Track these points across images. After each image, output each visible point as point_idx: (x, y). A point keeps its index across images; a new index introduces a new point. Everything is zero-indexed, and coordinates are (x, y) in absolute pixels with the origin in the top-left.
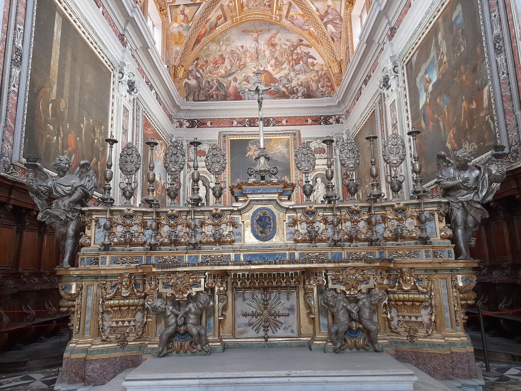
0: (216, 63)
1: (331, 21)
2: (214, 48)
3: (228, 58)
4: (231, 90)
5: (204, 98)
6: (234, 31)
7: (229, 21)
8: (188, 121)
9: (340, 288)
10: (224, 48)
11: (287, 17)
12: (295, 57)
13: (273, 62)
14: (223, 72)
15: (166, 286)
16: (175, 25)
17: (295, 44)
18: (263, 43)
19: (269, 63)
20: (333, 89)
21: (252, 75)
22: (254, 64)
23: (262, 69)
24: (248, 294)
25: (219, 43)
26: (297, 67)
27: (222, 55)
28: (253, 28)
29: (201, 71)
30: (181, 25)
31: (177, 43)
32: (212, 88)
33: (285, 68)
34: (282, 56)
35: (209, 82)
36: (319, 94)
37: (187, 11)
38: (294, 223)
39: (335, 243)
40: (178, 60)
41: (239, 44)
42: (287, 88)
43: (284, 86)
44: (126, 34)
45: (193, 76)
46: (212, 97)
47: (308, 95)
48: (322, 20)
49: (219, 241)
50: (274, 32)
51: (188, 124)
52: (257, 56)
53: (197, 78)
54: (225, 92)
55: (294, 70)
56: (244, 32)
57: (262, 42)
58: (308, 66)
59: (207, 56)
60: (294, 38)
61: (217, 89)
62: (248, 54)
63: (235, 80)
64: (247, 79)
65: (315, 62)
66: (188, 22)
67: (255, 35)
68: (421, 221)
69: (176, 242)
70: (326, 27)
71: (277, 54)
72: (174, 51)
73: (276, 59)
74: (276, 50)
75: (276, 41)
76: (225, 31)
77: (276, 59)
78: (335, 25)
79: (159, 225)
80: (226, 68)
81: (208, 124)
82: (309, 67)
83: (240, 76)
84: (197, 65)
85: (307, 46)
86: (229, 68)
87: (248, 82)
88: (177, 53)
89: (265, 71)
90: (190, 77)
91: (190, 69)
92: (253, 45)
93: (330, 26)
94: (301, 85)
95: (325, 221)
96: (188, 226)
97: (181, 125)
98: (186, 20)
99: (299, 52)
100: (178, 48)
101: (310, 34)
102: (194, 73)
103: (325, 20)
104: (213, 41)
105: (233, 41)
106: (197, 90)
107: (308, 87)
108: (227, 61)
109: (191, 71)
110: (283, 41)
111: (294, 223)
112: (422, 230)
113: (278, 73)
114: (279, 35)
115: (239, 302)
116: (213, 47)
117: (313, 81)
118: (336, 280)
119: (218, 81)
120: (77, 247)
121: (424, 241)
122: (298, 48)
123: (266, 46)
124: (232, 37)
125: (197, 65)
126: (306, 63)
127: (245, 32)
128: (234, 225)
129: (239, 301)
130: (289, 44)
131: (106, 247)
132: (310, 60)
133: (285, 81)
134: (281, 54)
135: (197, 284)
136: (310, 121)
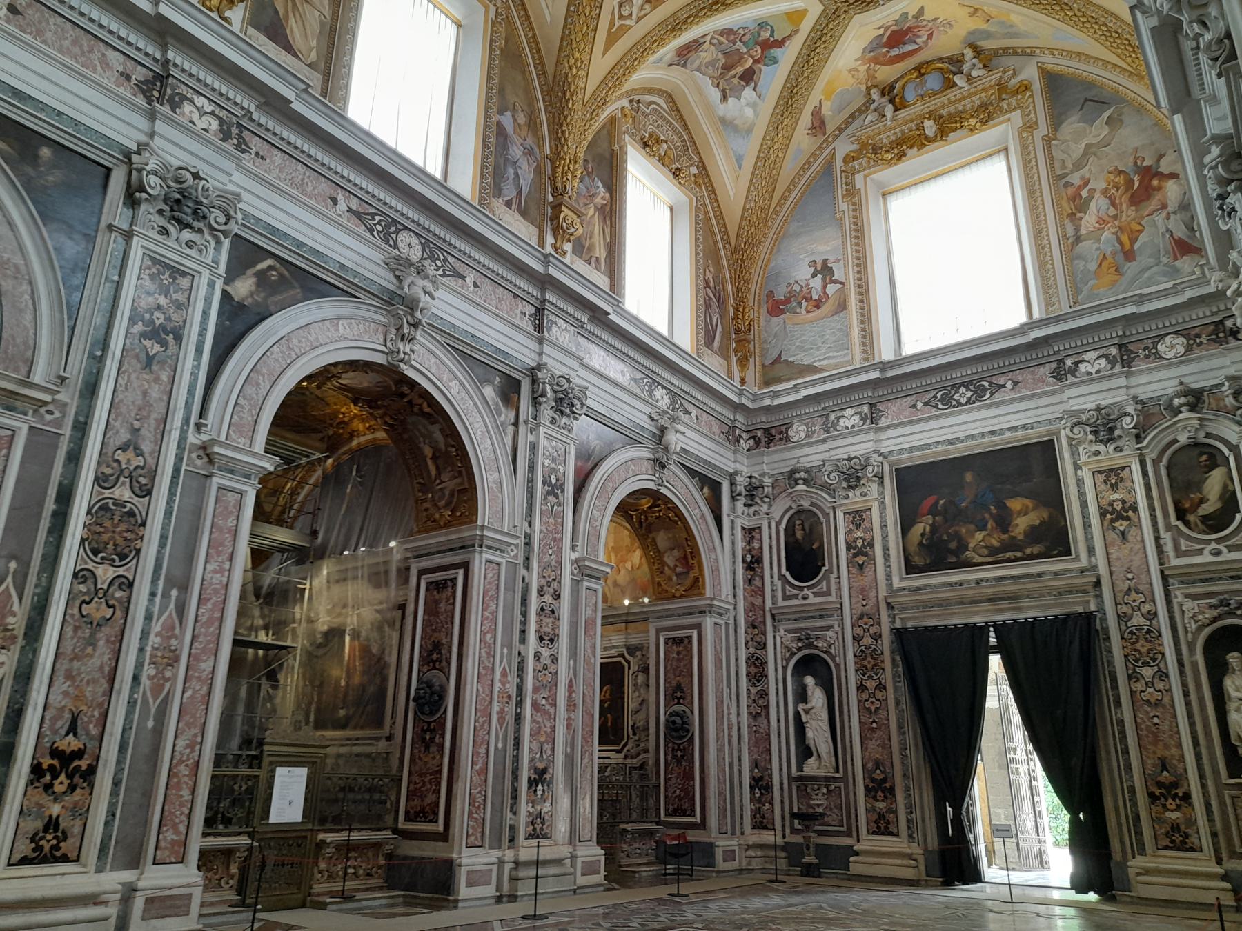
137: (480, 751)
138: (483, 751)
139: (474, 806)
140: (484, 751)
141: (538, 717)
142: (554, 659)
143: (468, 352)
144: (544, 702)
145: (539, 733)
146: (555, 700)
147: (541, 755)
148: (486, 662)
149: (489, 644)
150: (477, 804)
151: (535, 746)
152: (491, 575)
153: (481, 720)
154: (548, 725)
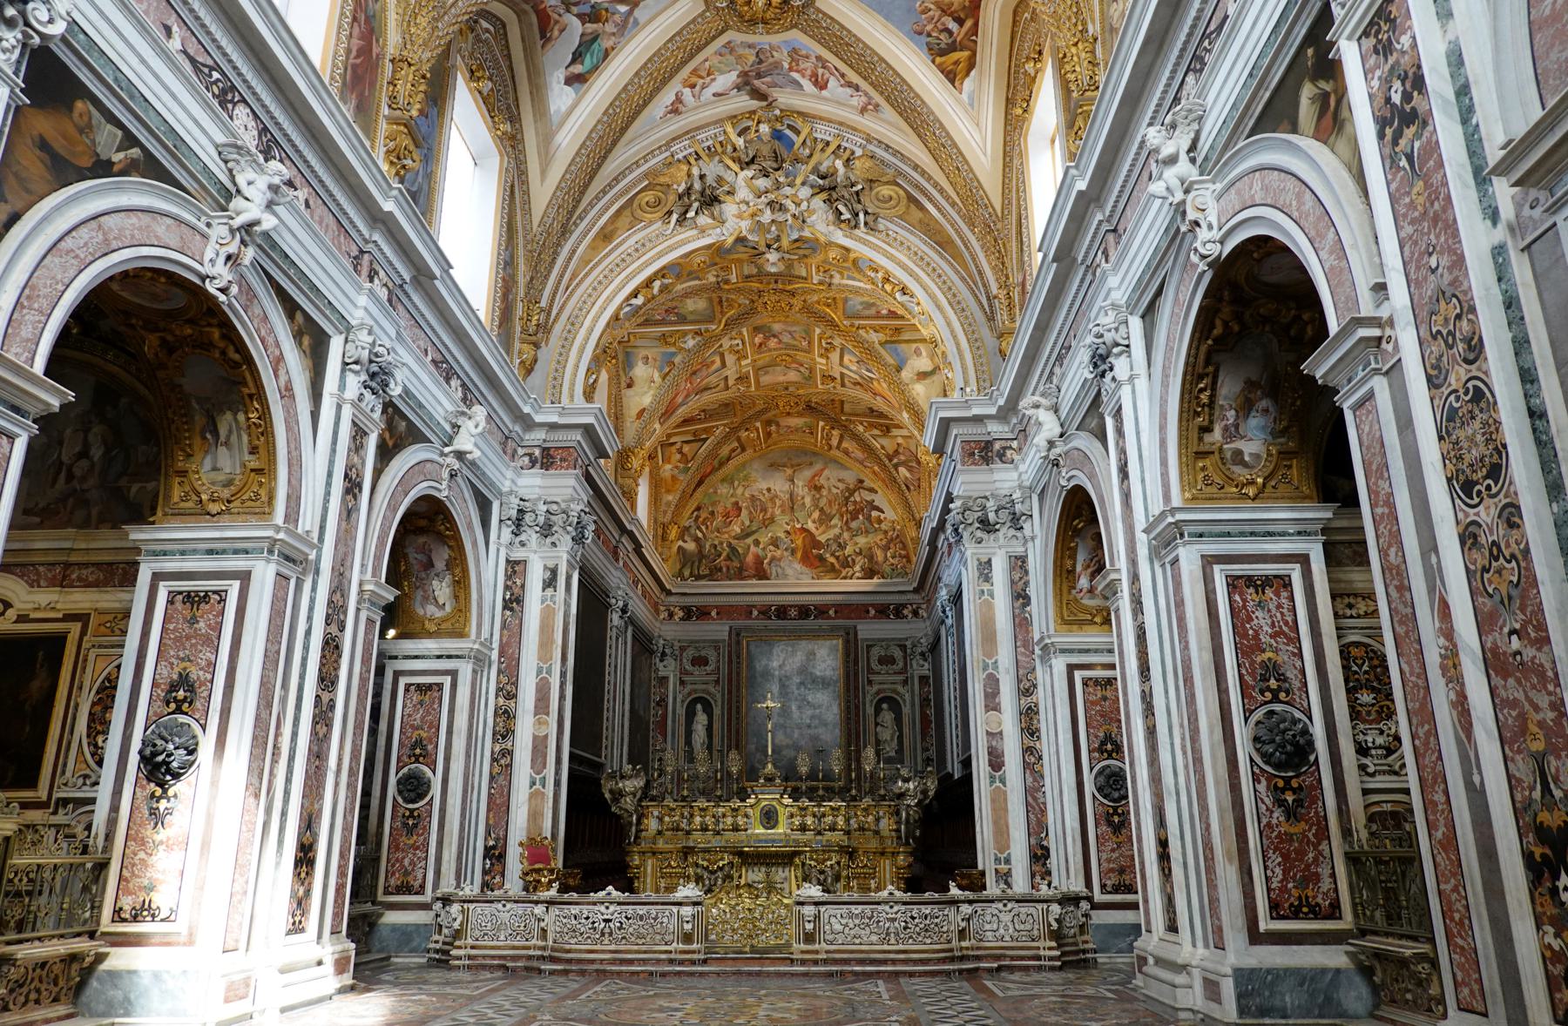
0: (727, 515)
1: (904, 464)
2: (725, 491)
3: (747, 508)
4: (750, 559)
5: (707, 572)
6: (756, 465)
7: (749, 451)
8: (682, 608)
9: (813, 863)
10: (740, 491)
11: (838, 448)
12: (851, 508)
13: (816, 515)
14: (738, 530)
15: (704, 860)
16: (668, 467)
17: (851, 486)
18: (801, 484)
19: (810, 516)
20: (909, 561)
21: (782, 535)
22: (787, 518)
23: (799, 526)
24: (756, 869)
25: (733, 483)
26: (854, 525)
27: (737, 503)
28: (785, 460)
29: (703, 528)
30: (677, 467)
31: (668, 491)
32: (719, 556)
33: (835, 526)
34: (830, 505)
35: (715, 546)
36: (888, 569)
37: (686, 449)
38: (792, 816)
39: (819, 833)
40: (669, 515)
41: (764, 486)
42: (837, 558)
43: (832, 555)
44: (621, 546)
45: (690, 535)
46: (720, 570)
47: (869, 573)
48: (890, 460)
49: (736, 829)
50: (818, 467)
51: (681, 614)
52: (792, 504)
53: (697, 540)
54: (741, 562)
55: (849, 529)
56: (772, 465)
57: (799, 483)
58: (870, 522)
59: (714, 504)
60: (850, 477)
61: (728, 558)
62: (778, 503)
63: (757, 543)
64: (775, 543)
65: (882, 516)
66: (688, 462)
67: (789, 471)
68: (878, 820)
69: (704, 829)
70: (896, 470)
71: (823, 502)
72: (664, 501)
73: (822, 510)
74: (821, 496)
75: (822, 481)
76: (744, 465)
77: (822, 510)
78: (910, 469)
79: (692, 816)
80: (743, 523)
81: (714, 613)
82: (872, 526)
83: (764, 539)
84: (698, 517)
85: (872, 490)
86: (747, 523)
87: (777, 547)
88: (668, 504)
89: (804, 530)
90: (686, 538)
91: (687, 524)
92: (787, 487)
93: (902, 470)
94: (860, 554)
95: (814, 816)
96: (714, 816)
97: (671, 615)
98: (685, 459)
99: (858, 499)
100: (670, 498)
101: (874, 472)
102: (692, 531)
103: (895, 461)
104: (723, 480)
105: (755, 481)
106: (696, 559)
107: (871, 558)
108: (744, 513)
109: (687, 529)
110: (833, 481)
111: (792, 816)
112: (877, 825)
113: (824, 532)
114: (826, 472)
115: (750, 872)
116: (724, 490)
117: (879, 547)
118: (811, 859)
119: (730, 545)
120: (639, 831)
121: (877, 832)
122: (856, 494)
123: (806, 489)
124: (754, 474)
125: (698, 517)
126: (869, 518)
127: (774, 466)
128: (746, 816)
129: (750, 872)
130: (841, 486)
131: (660, 833)
132: (874, 514)
133: (834, 547)
134: (830, 502)
135: (722, 859)
136: (872, 612)
137: (1436, 798)
138: (1440, 797)
139: (1452, 919)
140: (1443, 799)
141: (1512, 690)
142: (1511, 515)
143: (1268, 94)
144: (1515, 643)
145: (1523, 730)
146: (1542, 627)
147: (1546, 789)
148: (1400, 607)
149: (1398, 566)
150: (1457, 916)
151: (1524, 769)
152: (1367, 429)
153: (1421, 732)
154: (1543, 701)
